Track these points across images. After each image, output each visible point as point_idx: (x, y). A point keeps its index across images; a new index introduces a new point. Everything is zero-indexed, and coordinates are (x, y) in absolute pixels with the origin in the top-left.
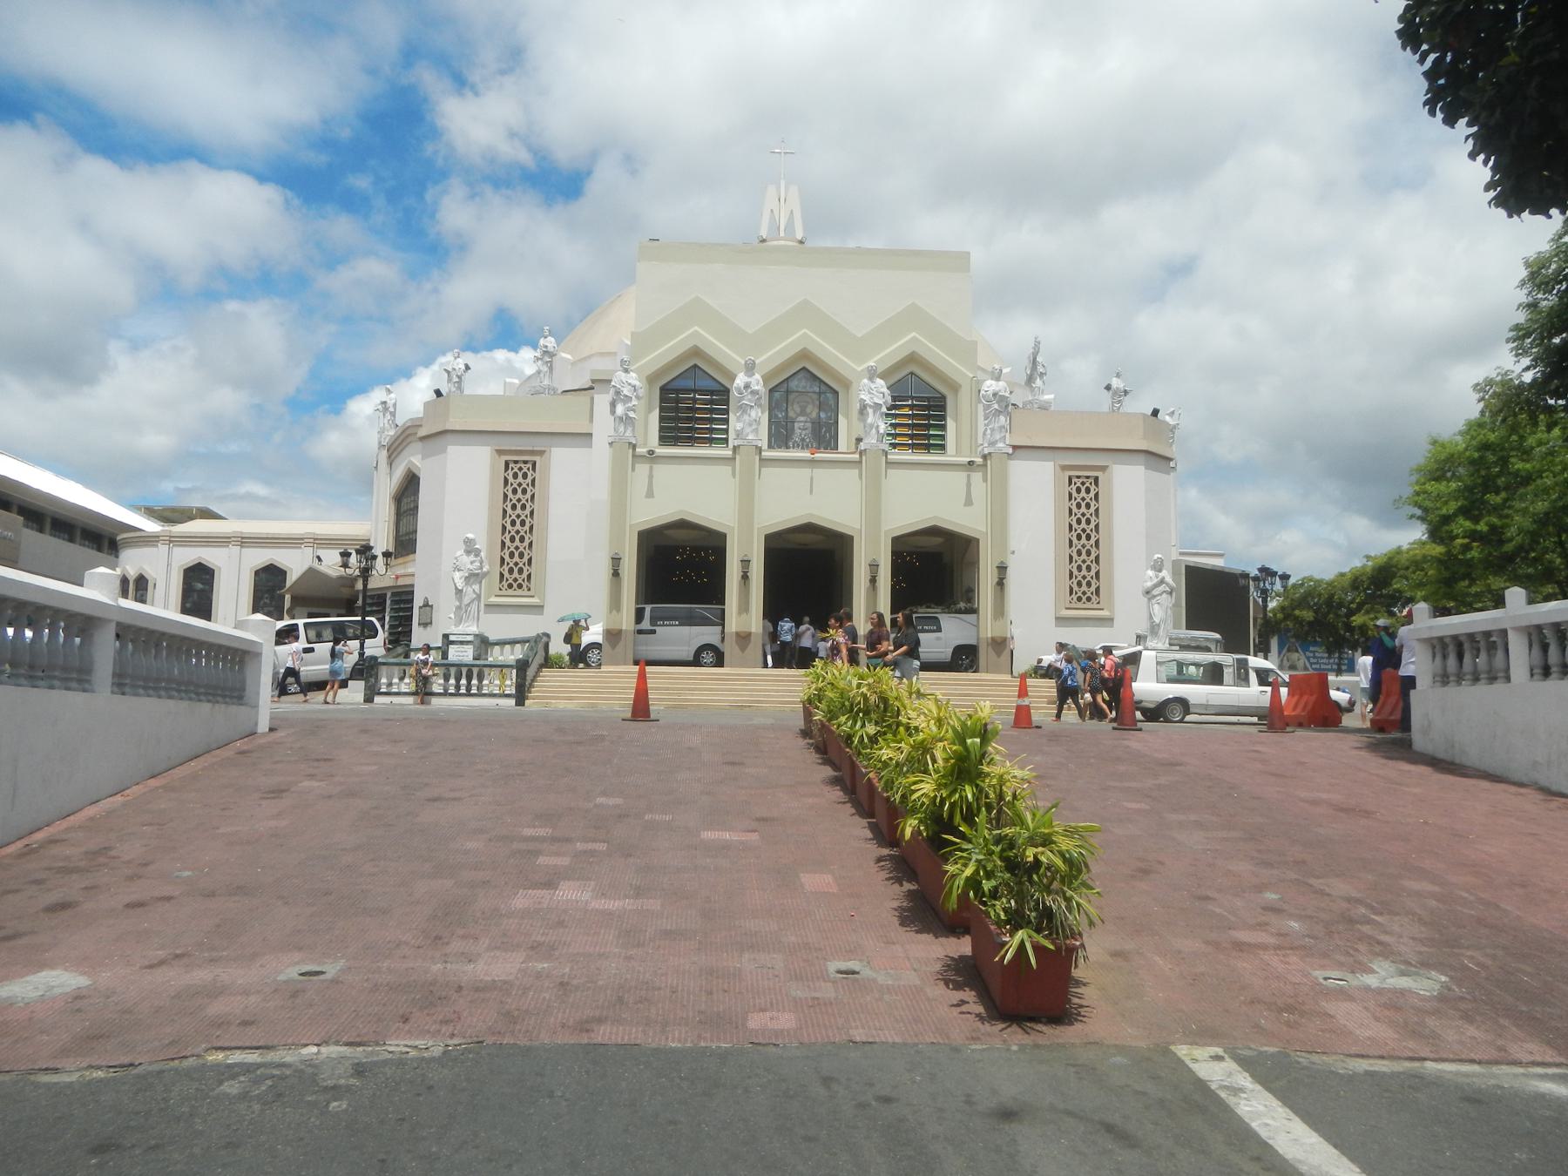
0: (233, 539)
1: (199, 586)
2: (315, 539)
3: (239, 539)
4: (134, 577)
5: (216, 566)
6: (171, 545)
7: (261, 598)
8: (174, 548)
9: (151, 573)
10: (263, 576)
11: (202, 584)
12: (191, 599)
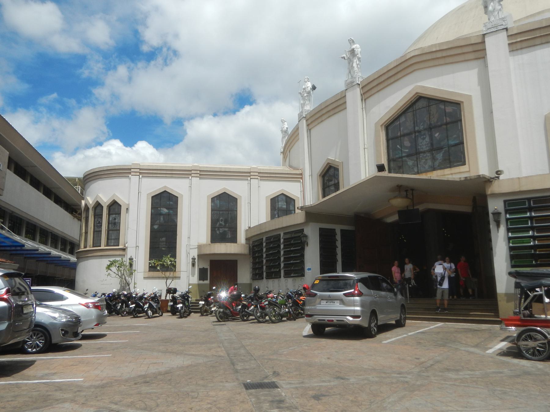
0: (193, 172)
1: (165, 211)
2: (259, 173)
3: (198, 172)
4: (107, 204)
5: (180, 194)
6: (141, 176)
7: (218, 220)
8: (143, 179)
9: (122, 199)
10: (218, 202)
11: (167, 208)
12: (158, 221)
